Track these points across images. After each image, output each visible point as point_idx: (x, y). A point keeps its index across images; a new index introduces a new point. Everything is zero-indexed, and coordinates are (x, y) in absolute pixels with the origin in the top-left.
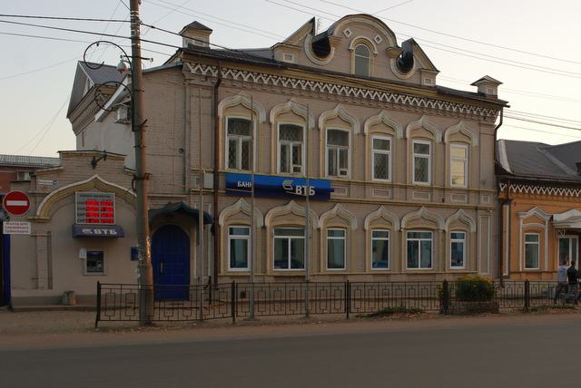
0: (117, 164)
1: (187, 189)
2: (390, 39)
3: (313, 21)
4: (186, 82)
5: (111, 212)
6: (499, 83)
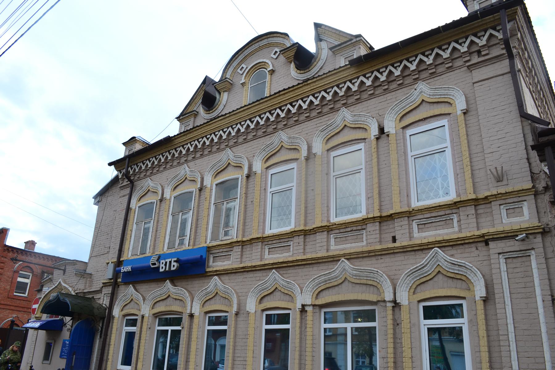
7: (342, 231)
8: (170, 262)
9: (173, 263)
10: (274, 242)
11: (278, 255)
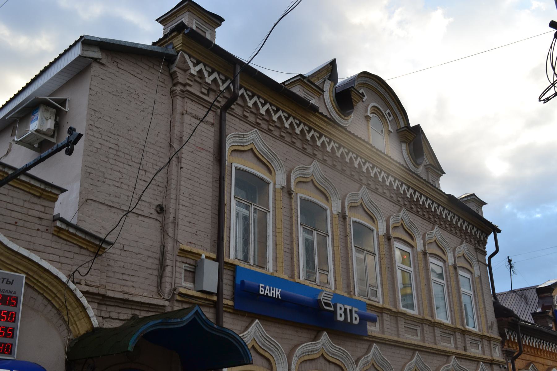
0: (37, 207)
1: (167, 288)
2: (400, 117)
3: (333, 63)
4: (175, 89)
5: (10, 325)
6: (484, 203)
7: (444, 331)
8: (351, 311)
9: (355, 315)
10: (410, 322)
11: (410, 337)
